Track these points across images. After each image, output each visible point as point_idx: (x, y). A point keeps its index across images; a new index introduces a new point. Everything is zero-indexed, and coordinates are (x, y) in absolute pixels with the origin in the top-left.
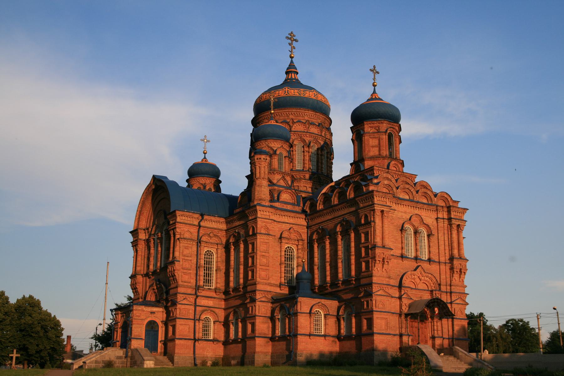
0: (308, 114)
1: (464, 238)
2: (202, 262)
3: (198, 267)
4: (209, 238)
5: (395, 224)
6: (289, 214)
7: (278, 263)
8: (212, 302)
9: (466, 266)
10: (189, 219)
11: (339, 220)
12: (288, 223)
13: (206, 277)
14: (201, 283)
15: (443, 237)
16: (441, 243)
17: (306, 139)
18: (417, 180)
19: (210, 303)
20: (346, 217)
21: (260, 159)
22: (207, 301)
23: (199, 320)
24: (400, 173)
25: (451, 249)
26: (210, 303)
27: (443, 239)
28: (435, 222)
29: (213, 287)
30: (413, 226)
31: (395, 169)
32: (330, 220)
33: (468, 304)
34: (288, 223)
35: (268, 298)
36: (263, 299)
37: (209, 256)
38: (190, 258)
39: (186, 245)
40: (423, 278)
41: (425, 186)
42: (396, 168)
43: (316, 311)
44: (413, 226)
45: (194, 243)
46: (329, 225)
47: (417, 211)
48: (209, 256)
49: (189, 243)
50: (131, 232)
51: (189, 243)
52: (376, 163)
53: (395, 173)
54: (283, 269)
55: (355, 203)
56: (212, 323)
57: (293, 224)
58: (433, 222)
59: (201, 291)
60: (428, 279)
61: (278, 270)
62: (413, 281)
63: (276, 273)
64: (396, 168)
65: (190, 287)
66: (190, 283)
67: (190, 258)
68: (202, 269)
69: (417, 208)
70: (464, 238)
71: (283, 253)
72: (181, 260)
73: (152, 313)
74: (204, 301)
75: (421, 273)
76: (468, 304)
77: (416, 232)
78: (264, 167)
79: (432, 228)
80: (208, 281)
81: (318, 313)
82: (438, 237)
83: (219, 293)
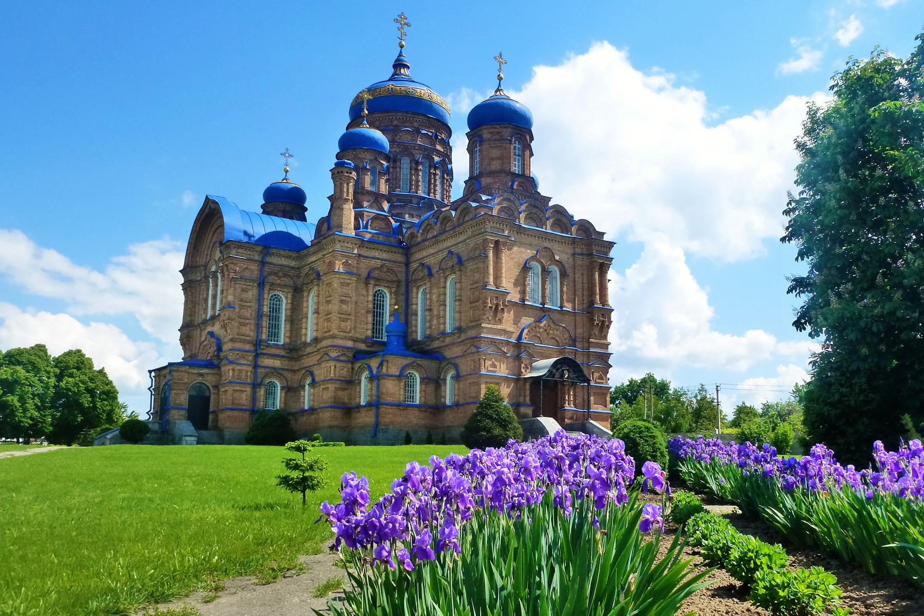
0: (418, 120)
1: (609, 280)
2: (266, 309)
3: (260, 315)
4: (276, 278)
5: (517, 260)
6: (381, 247)
7: (364, 311)
8: (279, 362)
9: (610, 318)
10: (249, 253)
12: (378, 259)
13: (272, 329)
14: (264, 337)
15: (581, 279)
16: (579, 286)
17: (414, 153)
18: (551, 204)
19: (277, 363)
21: (342, 172)
23: (260, 384)
24: (528, 194)
25: (592, 294)
26: (277, 363)
27: (581, 280)
28: (571, 259)
29: (282, 343)
30: (541, 263)
31: (521, 188)
32: (433, 254)
33: (611, 366)
34: (378, 259)
35: (348, 357)
36: (342, 358)
37: (277, 301)
38: (249, 304)
39: (245, 286)
40: (551, 332)
41: (560, 211)
42: (523, 187)
43: (410, 373)
44: (541, 263)
47: (547, 244)
48: (277, 301)
49: (248, 283)
50: (180, 271)
51: (248, 283)
52: (497, 180)
53: (521, 194)
54: (370, 319)
56: (279, 388)
57: (386, 260)
58: (568, 259)
59: (265, 347)
60: (558, 333)
61: (363, 319)
62: (539, 336)
63: (361, 324)
64: (523, 187)
66: (248, 336)
67: (249, 304)
68: (264, 319)
69: (547, 240)
70: (609, 280)
71: (371, 298)
72: (237, 306)
73: (201, 375)
74: (268, 360)
75: (549, 326)
76: (611, 366)
77: (545, 272)
78: (348, 184)
79: (567, 266)
80: (274, 334)
81: (411, 376)
82: (575, 278)
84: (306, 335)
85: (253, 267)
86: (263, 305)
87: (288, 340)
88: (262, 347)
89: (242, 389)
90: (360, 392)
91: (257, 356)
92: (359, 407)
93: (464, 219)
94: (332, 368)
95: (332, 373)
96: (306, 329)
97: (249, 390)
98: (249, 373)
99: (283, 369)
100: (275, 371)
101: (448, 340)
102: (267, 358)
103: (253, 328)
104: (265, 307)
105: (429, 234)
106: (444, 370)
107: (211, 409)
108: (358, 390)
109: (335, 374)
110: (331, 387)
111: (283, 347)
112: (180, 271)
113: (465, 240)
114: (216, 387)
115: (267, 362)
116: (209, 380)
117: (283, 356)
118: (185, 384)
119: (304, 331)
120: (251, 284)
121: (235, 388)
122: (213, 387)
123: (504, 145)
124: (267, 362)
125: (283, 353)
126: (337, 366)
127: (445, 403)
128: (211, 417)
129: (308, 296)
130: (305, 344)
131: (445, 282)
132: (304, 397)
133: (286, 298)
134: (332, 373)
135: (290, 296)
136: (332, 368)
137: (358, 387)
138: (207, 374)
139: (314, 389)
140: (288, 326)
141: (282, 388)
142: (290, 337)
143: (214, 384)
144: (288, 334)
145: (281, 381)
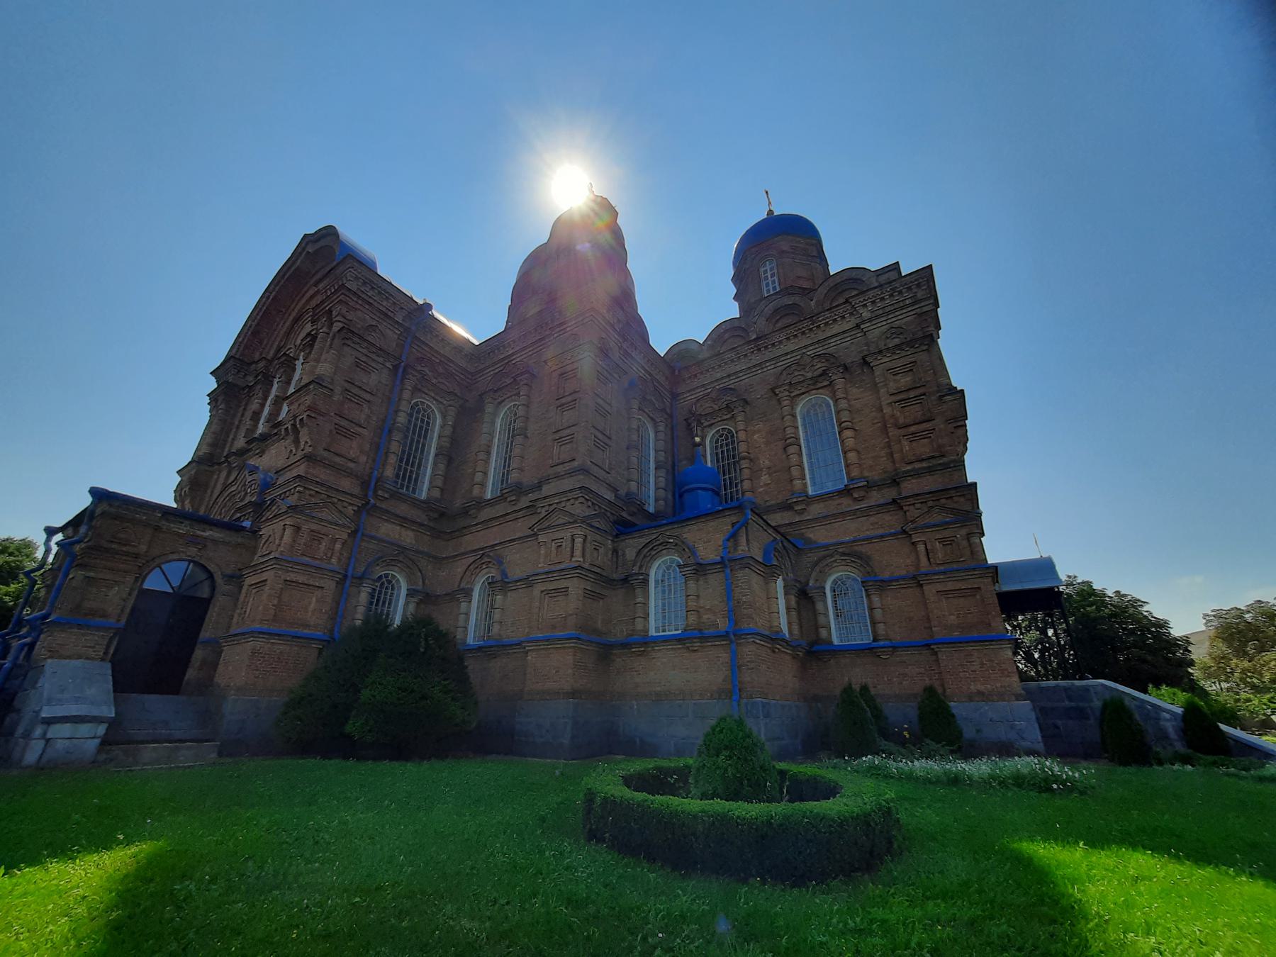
8: (411, 534)
11: (781, 364)
19: (407, 537)
20: (808, 353)
22: (398, 528)
26: (407, 537)
29: (424, 496)
38: (367, 396)
45: (388, 365)
46: (742, 383)
55: (843, 317)
56: (404, 592)
65: (350, 474)
67: (367, 396)
68: (397, 436)
72: (338, 390)
74: (390, 526)
83: (436, 515)
84: (483, 485)
85: (390, 333)
86: (397, 412)
87: (436, 493)
88: (380, 493)
89: (311, 582)
90: (646, 604)
91: (366, 508)
92: (646, 644)
93: (831, 304)
94: (579, 541)
95: (578, 553)
96: (485, 474)
97: (330, 585)
98: (338, 546)
99: (417, 552)
100: (400, 556)
101: (816, 510)
102: (386, 521)
103: (367, 447)
104: (402, 414)
105: (723, 348)
106: (817, 569)
107: (205, 634)
108: (640, 600)
109: (583, 555)
110: (576, 587)
111: (427, 505)
112: (211, 373)
113: (858, 326)
114: (236, 579)
115: (387, 530)
116: (221, 559)
117: (421, 525)
118: (137, 556)
119: (478, 478)
120: (381, 360)
121: (292, 576)
122: (224, 576)
123: (813, 264)
124: (387, 530)
125: (421, 517)
126: (589, 537)
127: (831, 643)
128: (199, 654)
129: (495, 415)
130: (481, 504)
131: (793, 407)
132: (467, 614)
133: (444, 417)
134: (578, 553)
135: (452, 412)
136: (579, 541)
137: (639, 591)
138: (214, 541)
139: (505, 595)
140: (442, 466)
141: (411, 594)
142: (442, 490)
143: (229, 572)
144: (439, 482)
145: (410, 581)
